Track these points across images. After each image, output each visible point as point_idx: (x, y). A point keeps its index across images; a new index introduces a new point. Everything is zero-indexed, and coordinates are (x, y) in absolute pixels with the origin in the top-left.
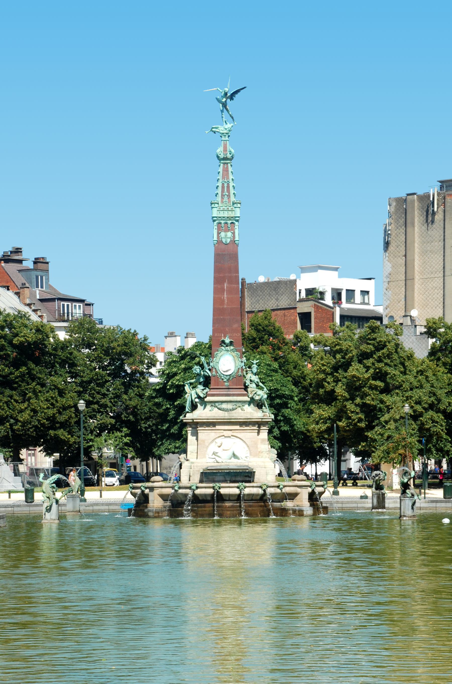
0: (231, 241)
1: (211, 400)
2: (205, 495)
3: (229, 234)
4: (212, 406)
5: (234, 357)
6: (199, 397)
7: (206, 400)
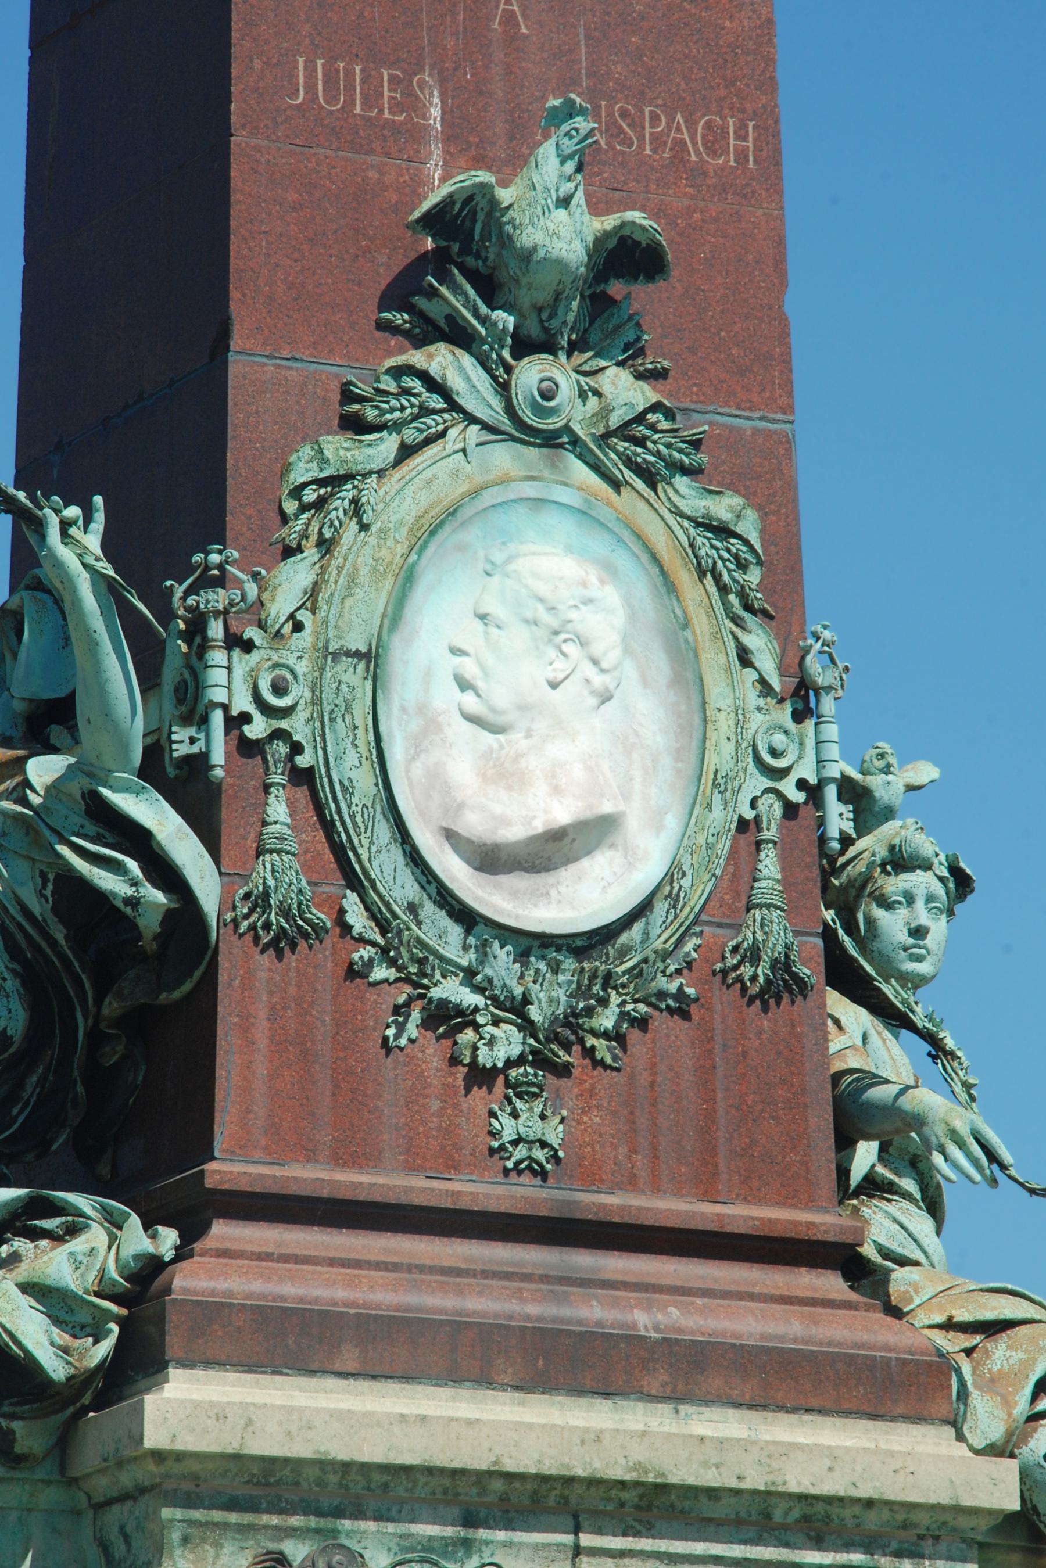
5: (670, 587)
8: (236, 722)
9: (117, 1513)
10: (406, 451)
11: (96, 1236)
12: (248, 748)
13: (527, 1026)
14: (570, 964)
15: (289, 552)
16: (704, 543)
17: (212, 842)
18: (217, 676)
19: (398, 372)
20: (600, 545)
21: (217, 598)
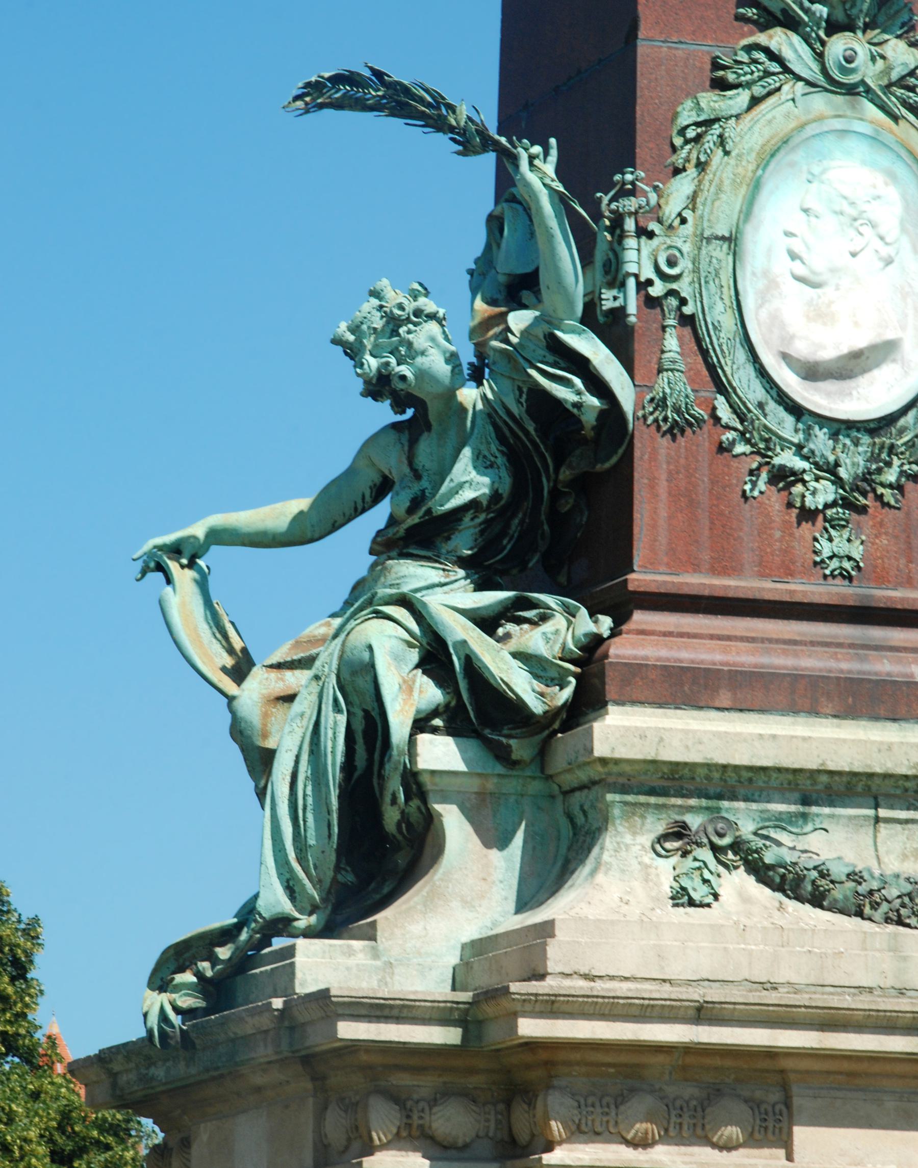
1: (673, 753)
4: (679, 832)
8: (643, 285)
9: (578, 798)
10: (755, 101)
11: (559, 621)
12: (651, 302)
13: (838, 481)
14: (866, 439)
15: (677, 171)
17: (628, 365)
18: (630, 255)
19: (749, 49)
20: (885, 159)
21: (630, 204)
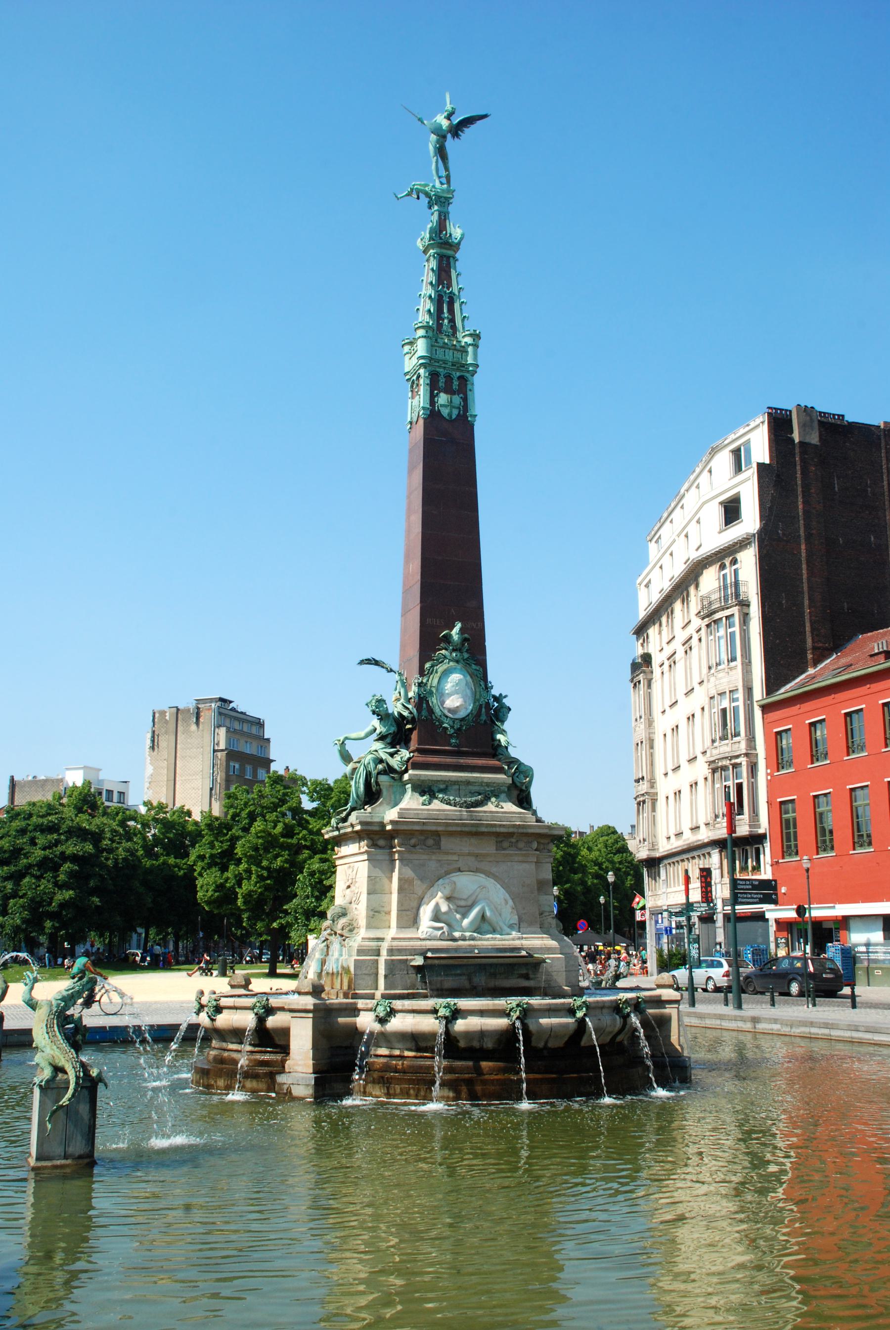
0: (459, 415)
2: (482, 1034)
3: (457, 399)
6: (389, 770)
7: (406, 777)
16: (475, 672)
